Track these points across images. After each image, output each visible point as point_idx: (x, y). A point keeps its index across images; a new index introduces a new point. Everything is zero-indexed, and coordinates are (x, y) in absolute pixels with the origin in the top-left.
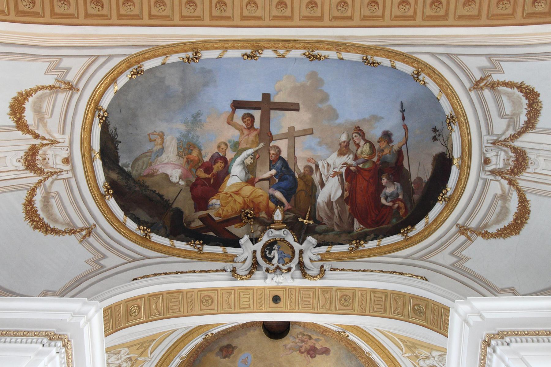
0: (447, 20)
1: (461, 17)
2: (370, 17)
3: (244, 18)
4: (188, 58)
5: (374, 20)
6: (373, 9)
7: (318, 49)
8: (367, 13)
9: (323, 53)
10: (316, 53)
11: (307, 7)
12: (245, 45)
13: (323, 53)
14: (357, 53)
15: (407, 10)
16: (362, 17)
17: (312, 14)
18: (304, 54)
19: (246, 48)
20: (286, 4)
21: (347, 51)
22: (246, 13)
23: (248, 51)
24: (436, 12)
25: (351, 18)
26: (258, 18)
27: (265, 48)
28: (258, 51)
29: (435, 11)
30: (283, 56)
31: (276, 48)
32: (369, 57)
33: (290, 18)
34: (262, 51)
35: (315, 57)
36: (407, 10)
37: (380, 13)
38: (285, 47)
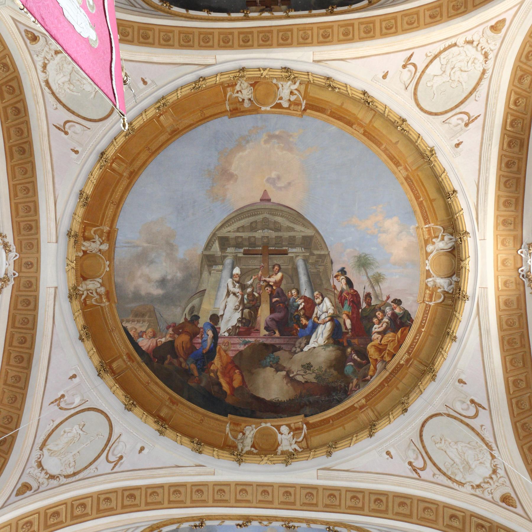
0: (388, 514)
1: (398, 514)
2: (330, 505)
3: (237, 501)
4: (196, 526)
5: (333, 508)
6: (332, 500)
7: (292, 522)
8: (328, 502)
9: (296, 524)
10: (291, 524)
11: (283, 495)
12: (238, 517)
13: (296, 524)
14: (322, 524)
15: (357, 503)
16: (324, 505)
17: (287, 500)
18: (282, 525)
19: (239, 520)
20: (268, 493)
21: (315, 523)
22: (239, 498)
23: (240, 522)
24: (379, 507)
25: (316, 505)
26: (248, 501)
27: (253, 520)
28: (247, 522)
29: (378, 506)
30: (266, 526)
31: (261, 520)
32: (331, 527)
33: (271, 502)
34: (251, 522)
35: (289, 527)
36: (357, 503)
37: (337, 503)
38: (268, 520)
